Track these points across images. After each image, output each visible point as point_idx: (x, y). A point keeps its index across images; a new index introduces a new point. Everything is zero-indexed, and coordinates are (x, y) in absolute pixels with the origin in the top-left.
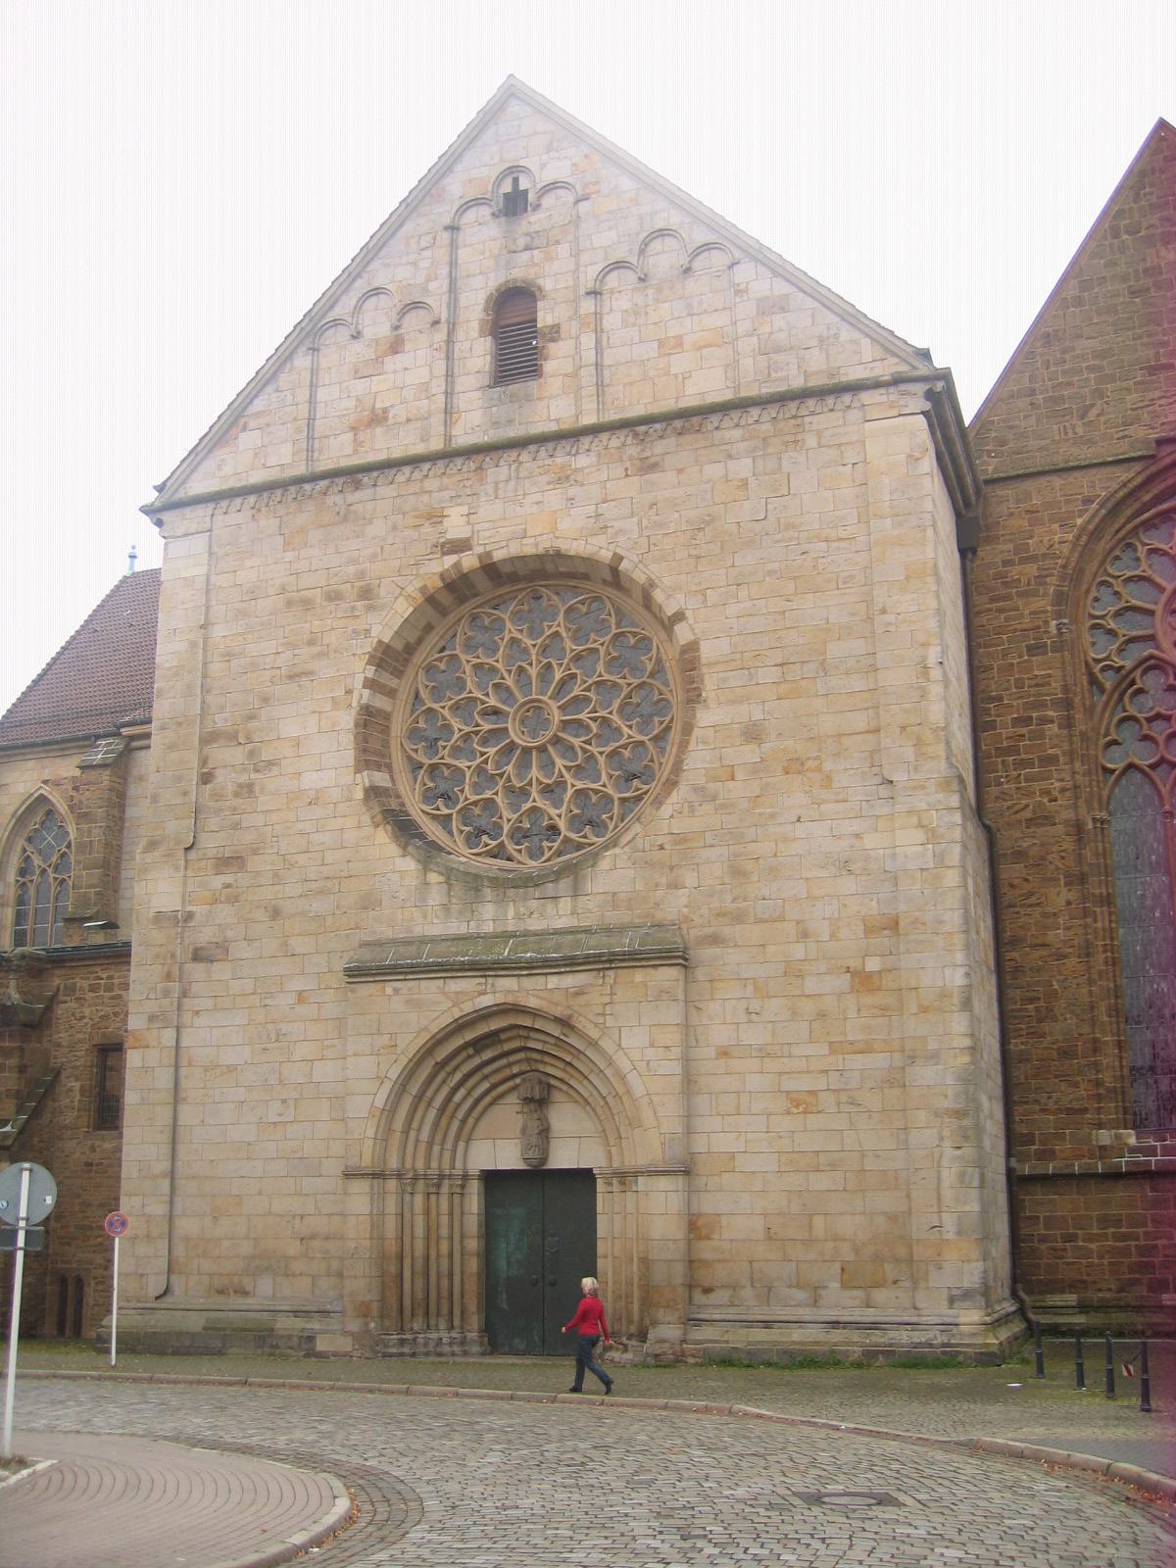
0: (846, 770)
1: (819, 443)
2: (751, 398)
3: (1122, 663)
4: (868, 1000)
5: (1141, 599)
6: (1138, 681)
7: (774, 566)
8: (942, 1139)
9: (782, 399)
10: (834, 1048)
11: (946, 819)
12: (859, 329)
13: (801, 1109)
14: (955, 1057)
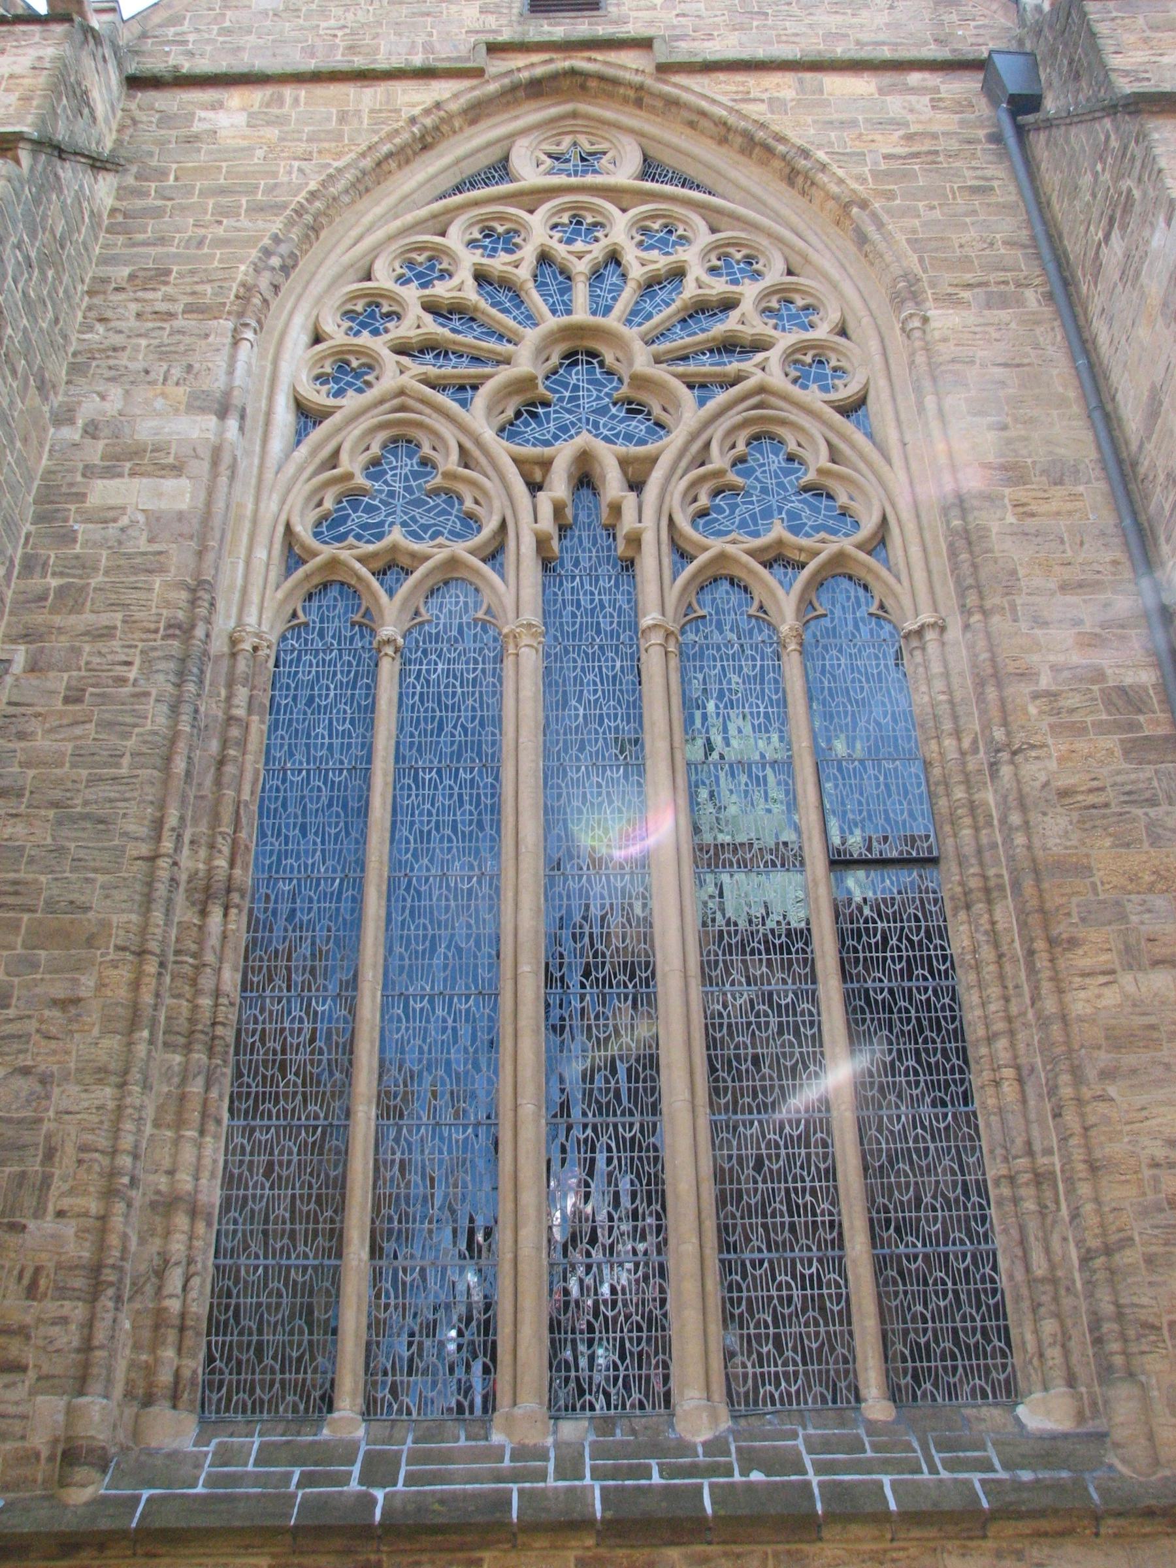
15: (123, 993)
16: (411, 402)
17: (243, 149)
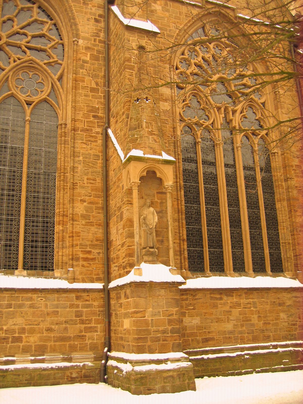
15: (176, 206)
16: (197, 89)
17: (163, 17)
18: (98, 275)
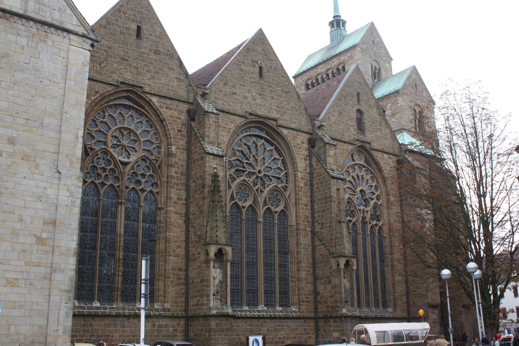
0: (44, 164)
1: (52, 45)
2: (32, 18)
3: (95, 148)
4: (41, 248)
5: (103, 129)
6: (99, 154)
7: (30, 82)
8: (61, 300)
9: (44, 23)
10: (27, 264)
11: (77, 190)
12: (73, 12)
13: (11, 285)
14: (69, 272)
18: (312, 309)
